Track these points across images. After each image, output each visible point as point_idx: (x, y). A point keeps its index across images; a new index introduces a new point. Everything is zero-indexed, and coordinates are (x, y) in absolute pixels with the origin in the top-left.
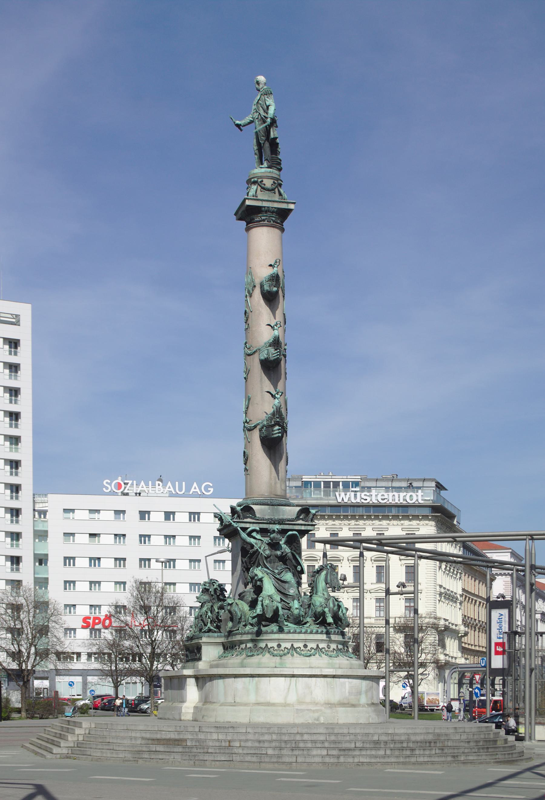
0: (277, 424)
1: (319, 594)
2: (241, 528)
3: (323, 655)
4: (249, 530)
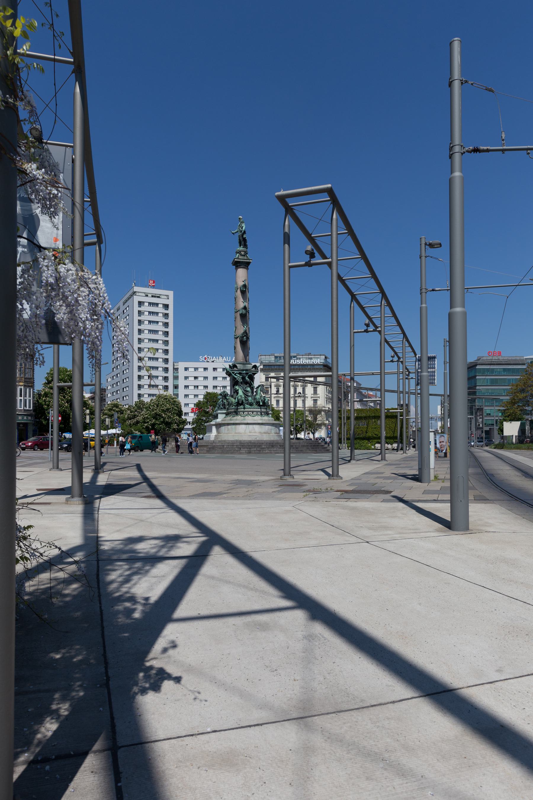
0: (245, 336)
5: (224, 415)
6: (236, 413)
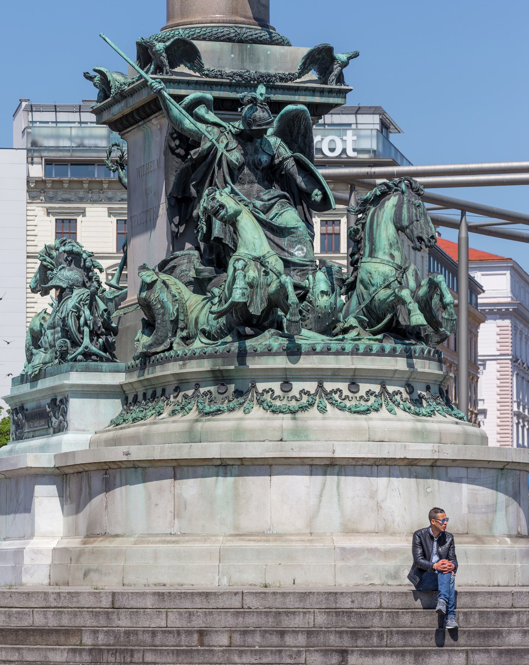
1: (381, 255)
2: (171, 95)
3: (399, 412)
4: (187, 100)
5: (112, 407)
6: (231, 385)
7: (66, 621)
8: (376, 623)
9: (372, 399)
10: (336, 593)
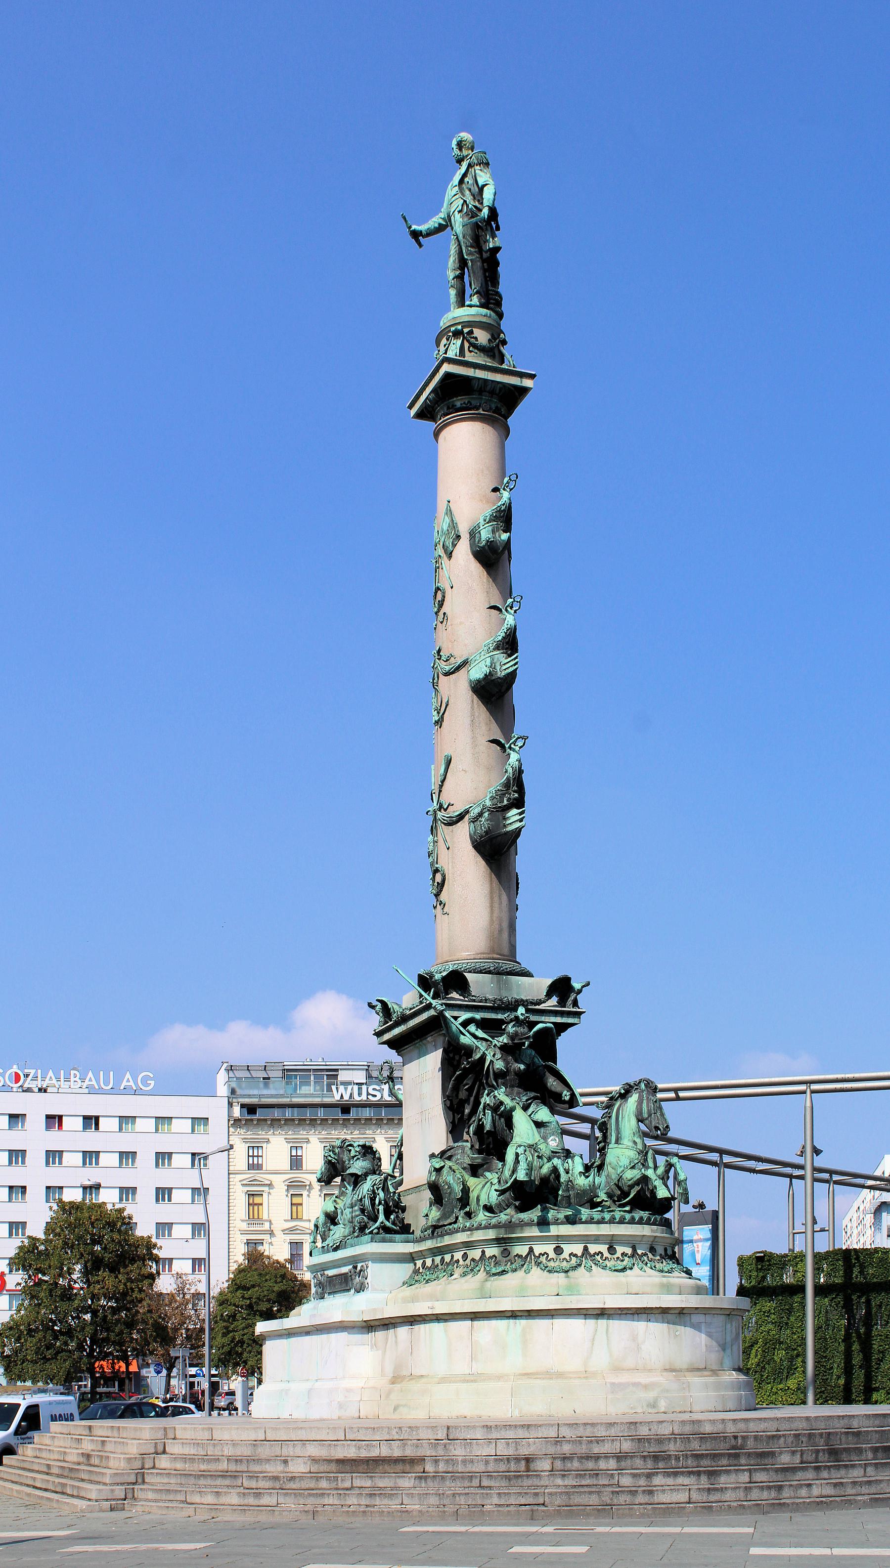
1: (626, 1141)
7: (409, 1452)
8: (672, 1448)
9: (626, 1259)
10: (636, 1423)
